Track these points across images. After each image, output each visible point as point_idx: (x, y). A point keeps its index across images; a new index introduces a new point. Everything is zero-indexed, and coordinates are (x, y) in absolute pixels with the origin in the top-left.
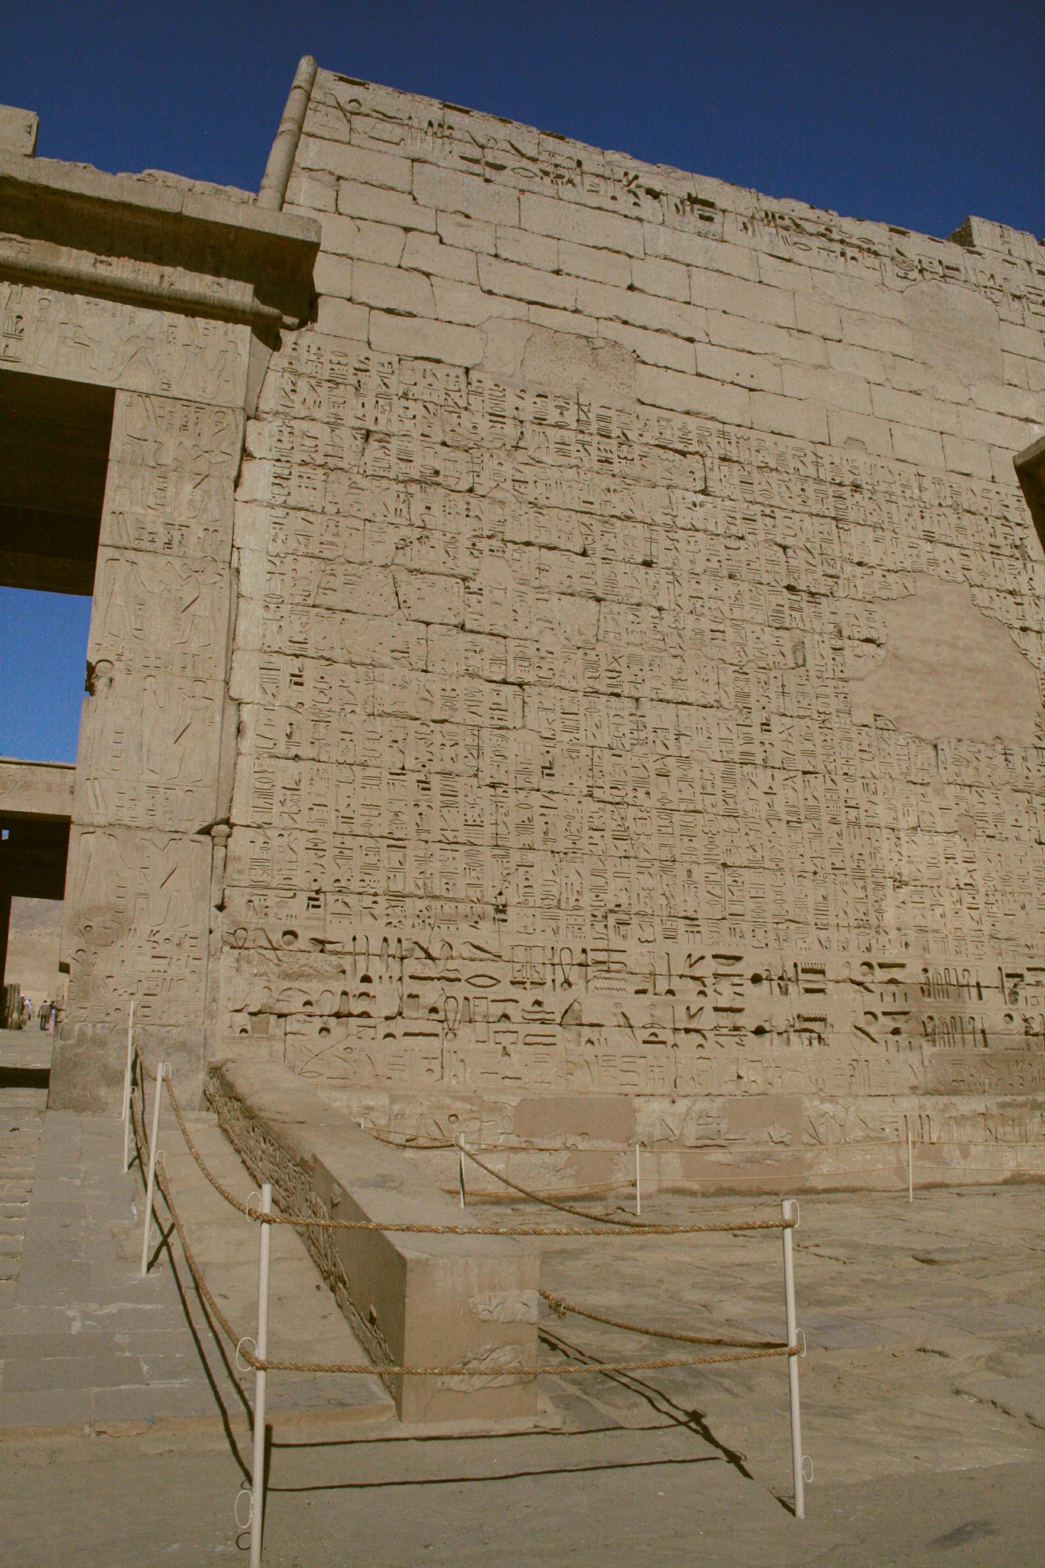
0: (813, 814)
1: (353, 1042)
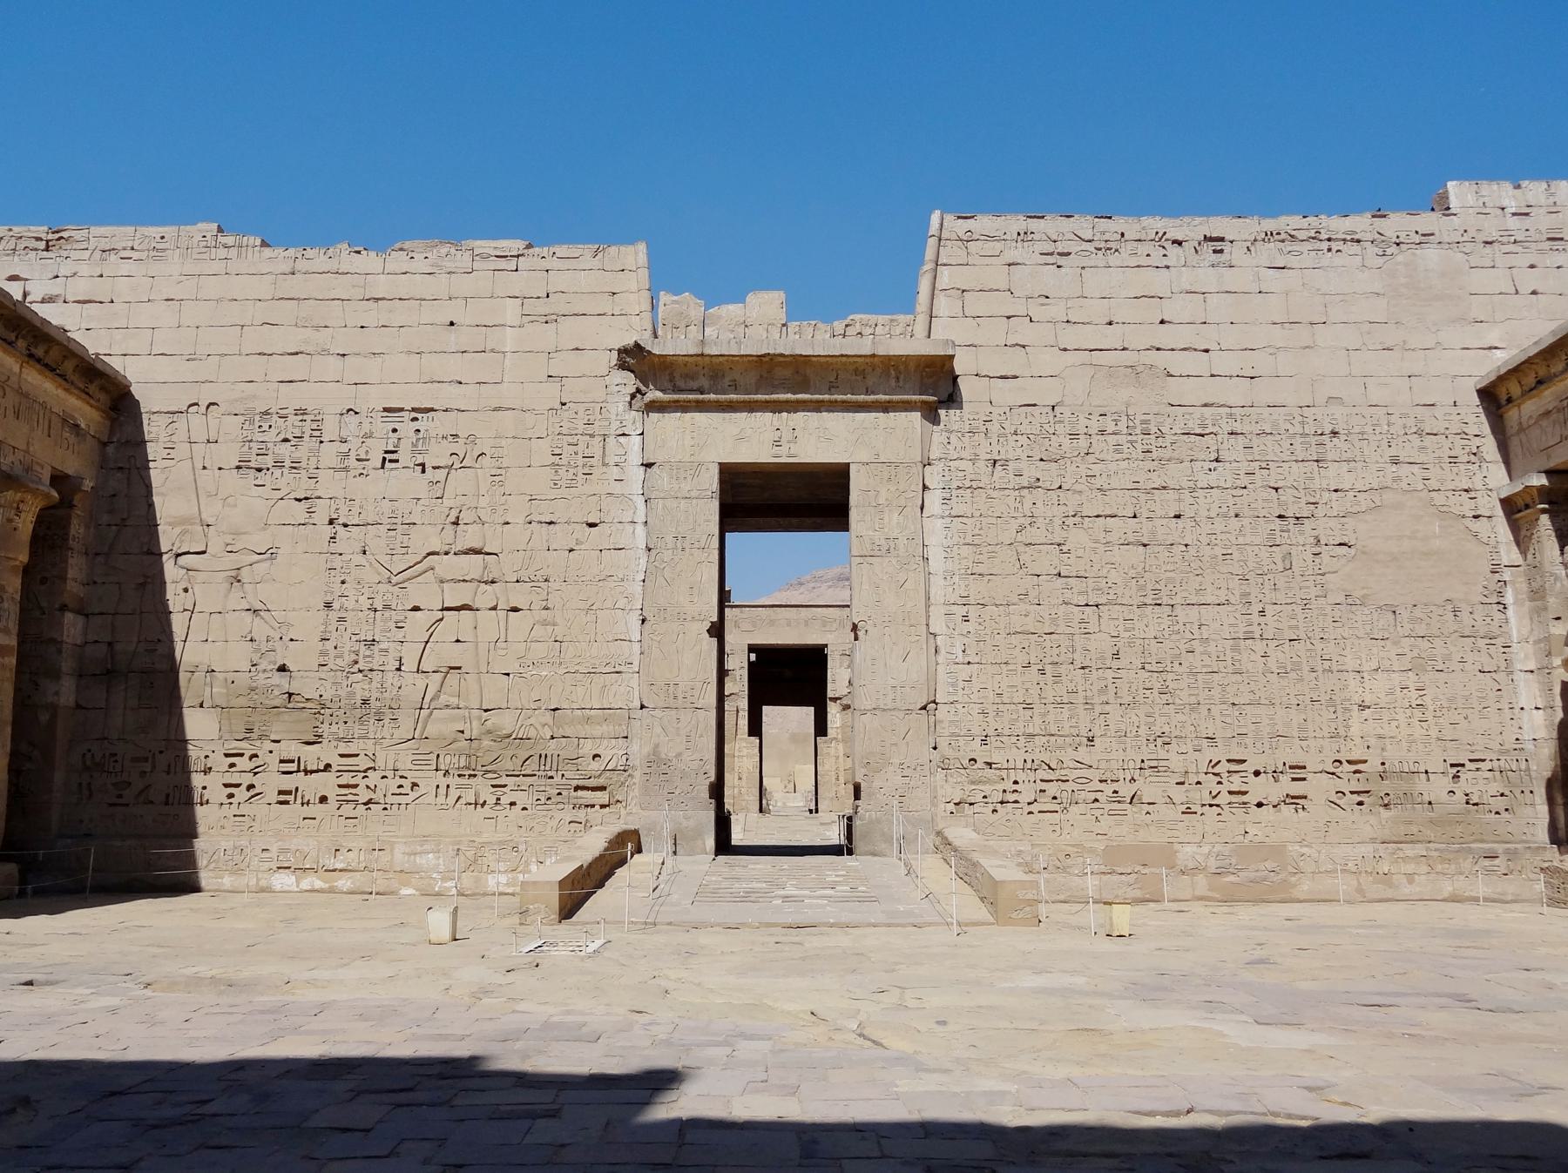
0: (1297, 667)
1: (1010, 816)
